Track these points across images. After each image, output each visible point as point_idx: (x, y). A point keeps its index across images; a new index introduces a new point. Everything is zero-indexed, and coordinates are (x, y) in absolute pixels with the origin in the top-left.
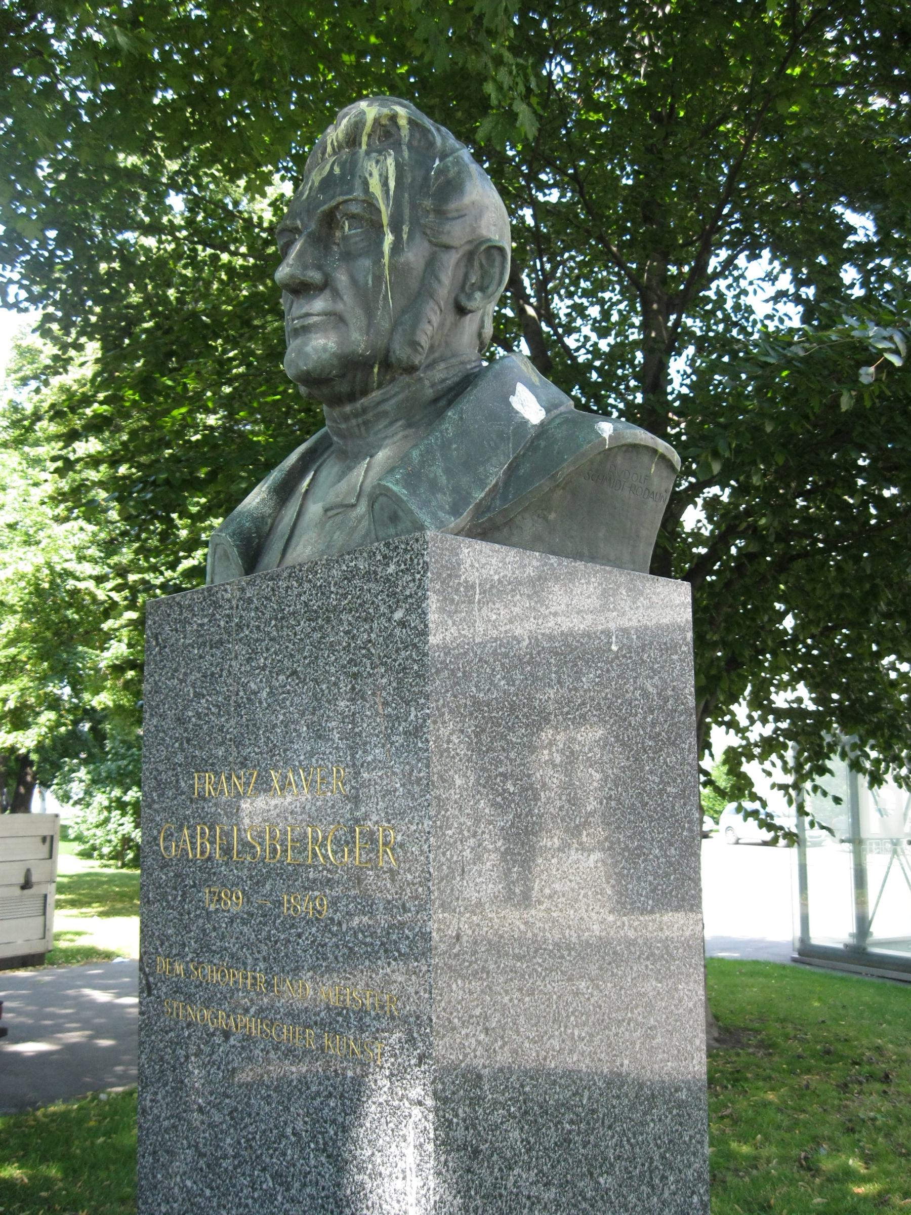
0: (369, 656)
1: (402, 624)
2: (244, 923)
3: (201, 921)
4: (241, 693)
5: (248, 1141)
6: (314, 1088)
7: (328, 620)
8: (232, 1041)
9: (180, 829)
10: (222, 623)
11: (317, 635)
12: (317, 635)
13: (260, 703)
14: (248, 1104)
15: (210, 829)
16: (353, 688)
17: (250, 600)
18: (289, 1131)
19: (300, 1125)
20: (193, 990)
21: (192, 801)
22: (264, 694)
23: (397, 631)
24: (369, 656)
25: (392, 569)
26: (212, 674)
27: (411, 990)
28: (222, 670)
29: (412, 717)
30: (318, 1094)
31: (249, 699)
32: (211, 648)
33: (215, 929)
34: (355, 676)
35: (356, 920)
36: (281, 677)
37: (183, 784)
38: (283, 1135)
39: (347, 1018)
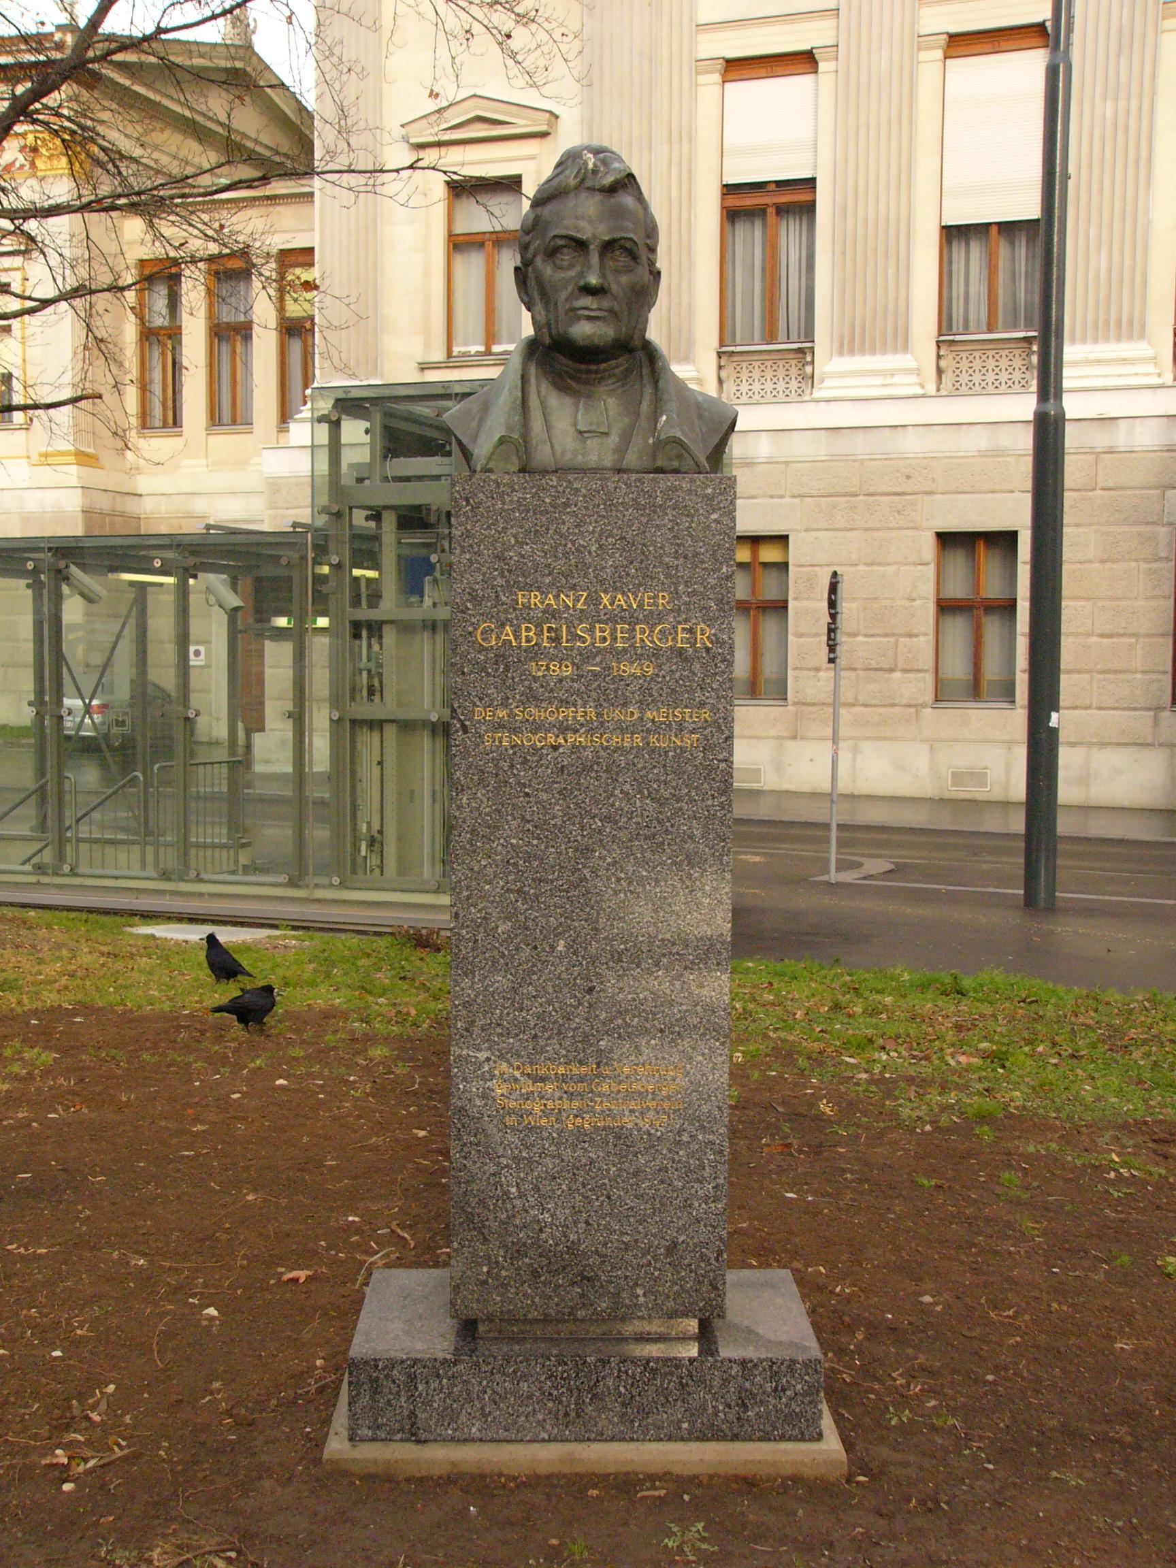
0: (690, 535)
1: (717, 521)
2: (573, 680)
3: (526, 683)
4: (570, 545)
5: (577, 804)
6: (640, 766)
7: (655, 512)
8: (561, 750)
9: (503, 625)
10: (547, 500)
11: (644, 520)
12: (644, 520)
13: (590, 553)
14: (578, 784)
15: (536, 627)
16: (677, 552)
17: (577, 490)
18: (617, 792)
19: (627, 787)
20: (518, 724)
21: (515, 609)
22: (594, 548)
23: (713, 525)
24: (690, 535)
25: (709, 491)
26: (536, 531)
27: (721, 706)
28: (548, 529)
29: (724, 570)
30: (645, 768)
31: (578, 550)
32: (535, 513)
33: (542, 686)
34: (678, 545)
35: (677, 675)
36: (610, 540)
37: (504, 599)
38: (612, 795)
39: (669, 726)
